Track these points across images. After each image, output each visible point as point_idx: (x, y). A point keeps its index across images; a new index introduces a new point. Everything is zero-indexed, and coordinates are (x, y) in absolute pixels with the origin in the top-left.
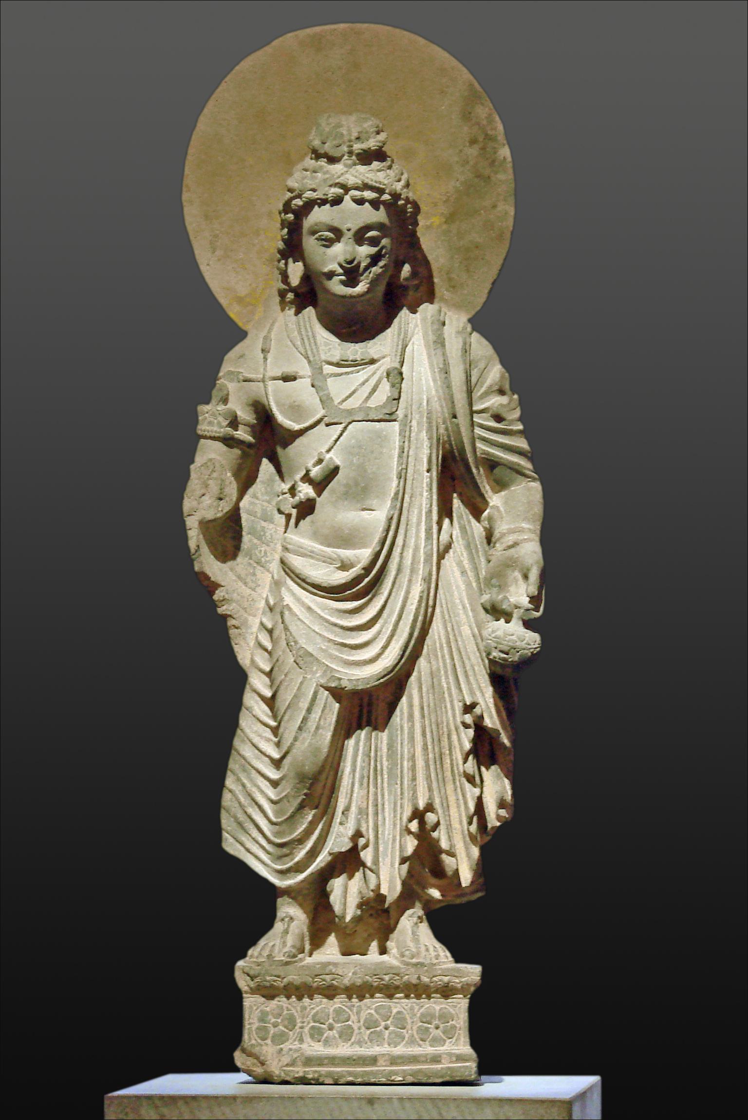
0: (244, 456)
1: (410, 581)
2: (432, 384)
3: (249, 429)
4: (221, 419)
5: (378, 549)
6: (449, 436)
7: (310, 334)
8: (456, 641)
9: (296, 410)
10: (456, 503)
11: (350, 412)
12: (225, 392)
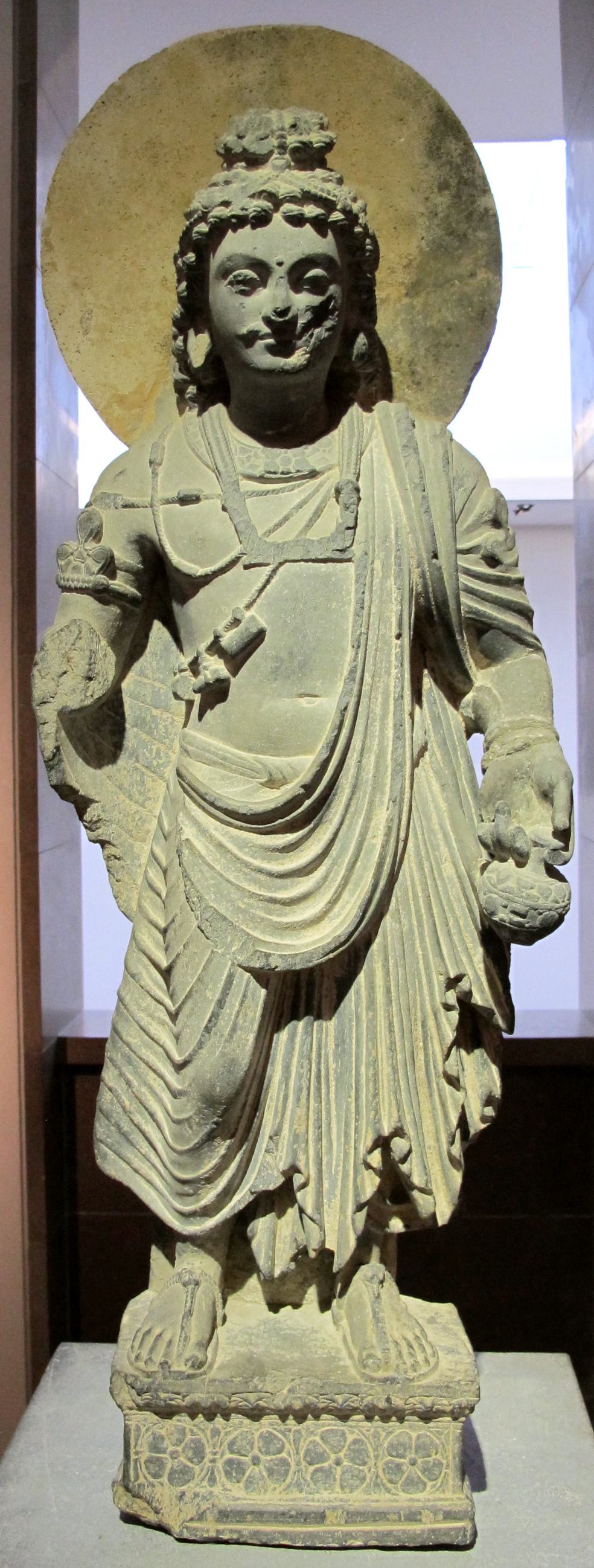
0: (125, 616)
1: (371, 803)
2: (401, 506)
3: (131, 577)
4: (90, 561)
5: (325, 756)
6: (425, 586)
7: (220, 436)
8: (436, 886)
9: (199, 545)
10: (427, 682)
11: (280, 547)
12: (97, 523)
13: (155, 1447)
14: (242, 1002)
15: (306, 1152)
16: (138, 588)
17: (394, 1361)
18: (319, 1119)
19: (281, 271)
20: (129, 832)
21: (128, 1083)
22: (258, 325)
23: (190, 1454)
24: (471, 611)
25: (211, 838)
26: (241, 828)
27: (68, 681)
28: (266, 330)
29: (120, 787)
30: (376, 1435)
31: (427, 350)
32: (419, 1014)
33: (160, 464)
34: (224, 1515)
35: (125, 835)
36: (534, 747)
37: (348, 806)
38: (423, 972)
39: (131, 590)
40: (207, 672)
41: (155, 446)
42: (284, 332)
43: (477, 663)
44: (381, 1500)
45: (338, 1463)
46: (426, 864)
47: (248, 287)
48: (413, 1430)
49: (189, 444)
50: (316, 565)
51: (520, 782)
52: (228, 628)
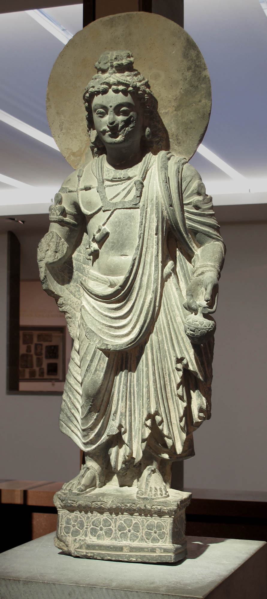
0: (71, 230)
1: (146, 293)
4: (57, 211)
7: (100, 166)
9: (89, 204)
11: (115, 204)
12: (60, 198)
13: (68, 522)
14: (99, 361)
15: (126, 420)
17: (148, 492)
18: (131, 408)
19: (111, 109)
20: (74, 308)
21: (70, 398)
22: (106, 128)
23: (79, 525)
25: (91, 305)
26: (101, 301)
27: (49, 253)
28: (108, 129)
29: (71, 292)
30: (143, 522)
31: (183, 131)
32: (167, 372)
34: (89, 547)
35: (73, 310)
37: (138, 294)
38: (168, 356)
39: (72, 221)
42: (114, 130)
44: (143, 544)
45: (129, 531)
46: (169, 317)
47: (102, 115)
48: (155, 520)
51: (200, 286)
52: (97, 233)
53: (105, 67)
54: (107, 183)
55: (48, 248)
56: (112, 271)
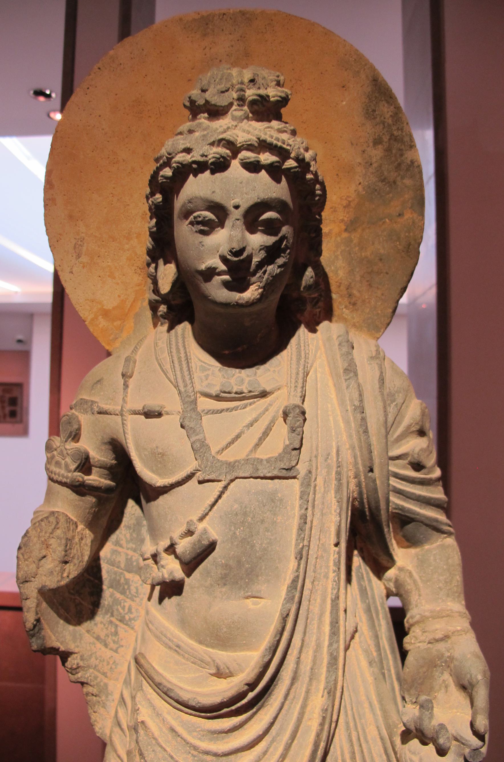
0: (101, 503)
1: (308, 692)
2: (342, 425)
3: (106, 472)
4: (68, 460)
5: (266, 659)
6: (361, 493)
7: (183, 355)
8: (362, 752)
9: (159, 459)
10: (357, 560)
11: (231, 466)
12: (76, 426)
16: (112, 480)
19: (237, 214)
20: (104, 674)
24: (398, 507)
26: (191, 714)
27: (49, 564)
28: (223, 267)
29: (98, 638)
31: (362, 277)
33: (131, 377)
35: (101, 677)
36: (453, 638)
40: (165, 571)
41: (128, 360)
42: (239, 271)
43: (398, 543)
47: (207, 228)
49: (157, 358)
50: (264, 481)
51: (440, 669)
53: (221, 101)
54: (204, 403)
55: (44, 553)
56: (223, 637)
